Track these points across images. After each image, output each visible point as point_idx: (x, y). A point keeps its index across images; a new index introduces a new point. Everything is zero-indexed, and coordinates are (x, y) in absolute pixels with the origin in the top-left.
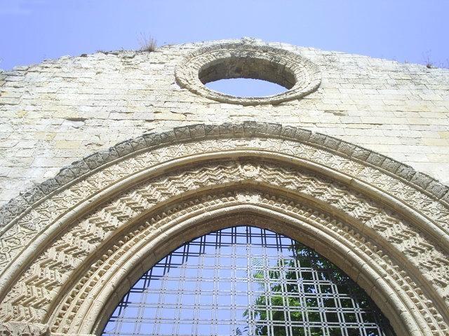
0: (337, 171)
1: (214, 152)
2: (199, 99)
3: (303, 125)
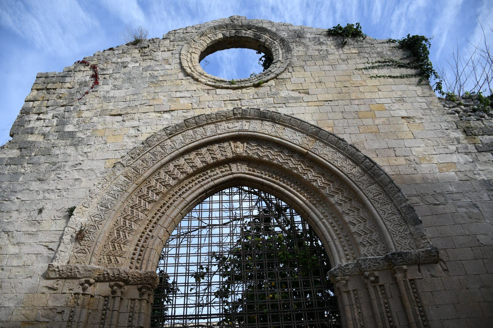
0: (297, 145)
1: (213, 136)
2: (200, 86)
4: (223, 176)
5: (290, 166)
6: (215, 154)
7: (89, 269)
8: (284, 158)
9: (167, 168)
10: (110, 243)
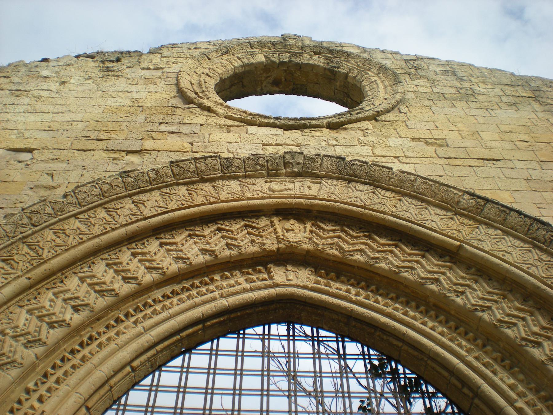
0: (435, 231)
1: (236, 200)
3: (379, 159)
4: (251, 290)
5: (419, 275)
6: (235, 239)
8: (402, 258)
9: (114, 256)
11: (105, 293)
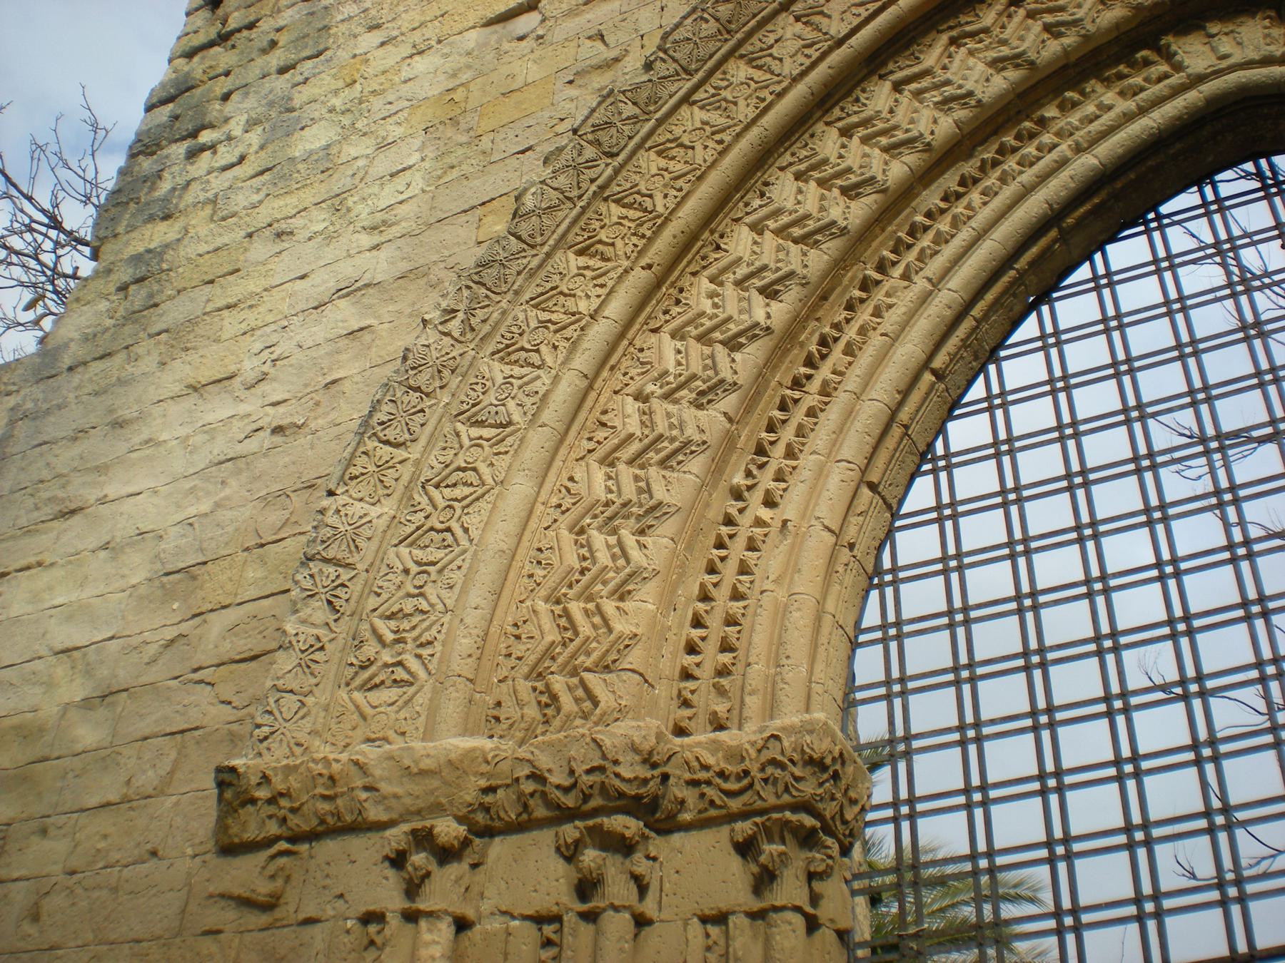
4: (1142, 111)
7: (426, 764)
9: (804, 153)
10: (541, 606)
11: (819, 237)
